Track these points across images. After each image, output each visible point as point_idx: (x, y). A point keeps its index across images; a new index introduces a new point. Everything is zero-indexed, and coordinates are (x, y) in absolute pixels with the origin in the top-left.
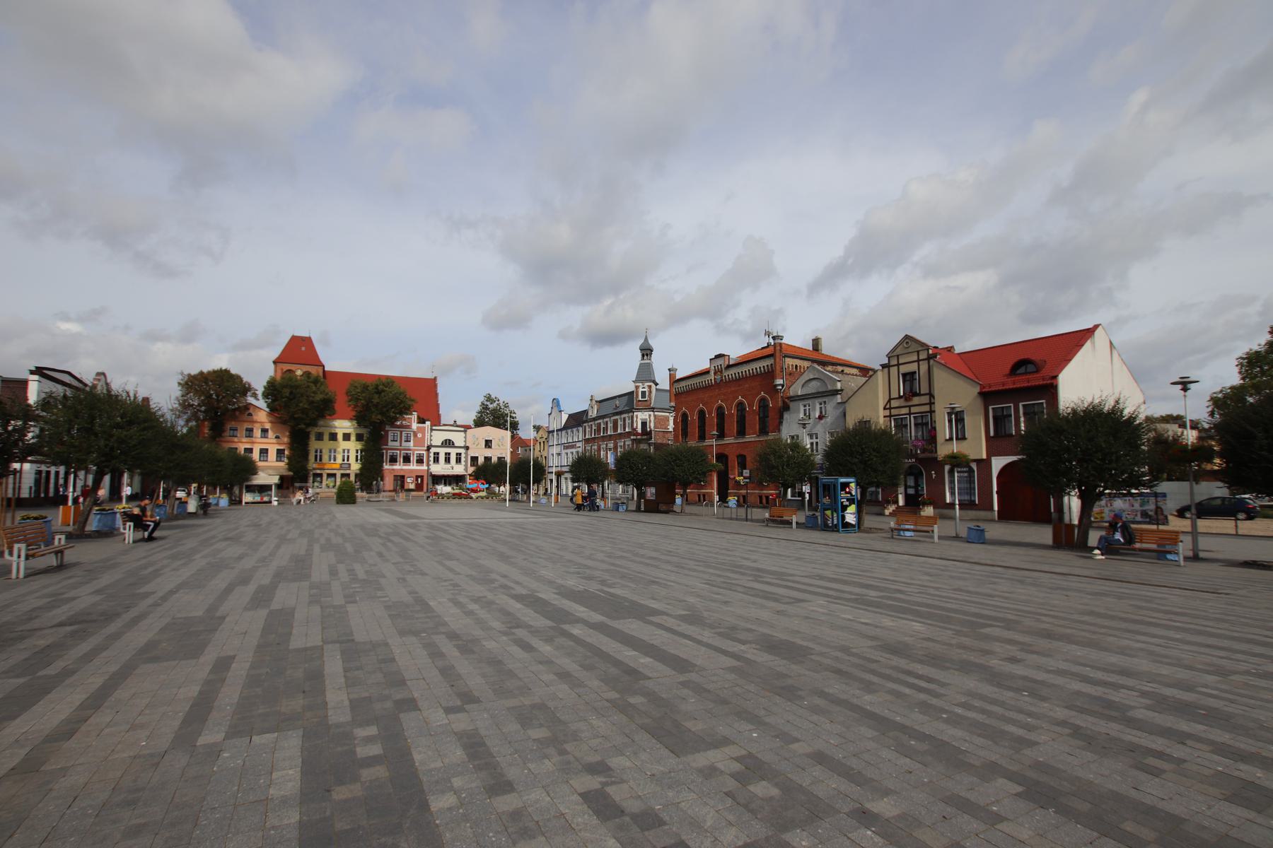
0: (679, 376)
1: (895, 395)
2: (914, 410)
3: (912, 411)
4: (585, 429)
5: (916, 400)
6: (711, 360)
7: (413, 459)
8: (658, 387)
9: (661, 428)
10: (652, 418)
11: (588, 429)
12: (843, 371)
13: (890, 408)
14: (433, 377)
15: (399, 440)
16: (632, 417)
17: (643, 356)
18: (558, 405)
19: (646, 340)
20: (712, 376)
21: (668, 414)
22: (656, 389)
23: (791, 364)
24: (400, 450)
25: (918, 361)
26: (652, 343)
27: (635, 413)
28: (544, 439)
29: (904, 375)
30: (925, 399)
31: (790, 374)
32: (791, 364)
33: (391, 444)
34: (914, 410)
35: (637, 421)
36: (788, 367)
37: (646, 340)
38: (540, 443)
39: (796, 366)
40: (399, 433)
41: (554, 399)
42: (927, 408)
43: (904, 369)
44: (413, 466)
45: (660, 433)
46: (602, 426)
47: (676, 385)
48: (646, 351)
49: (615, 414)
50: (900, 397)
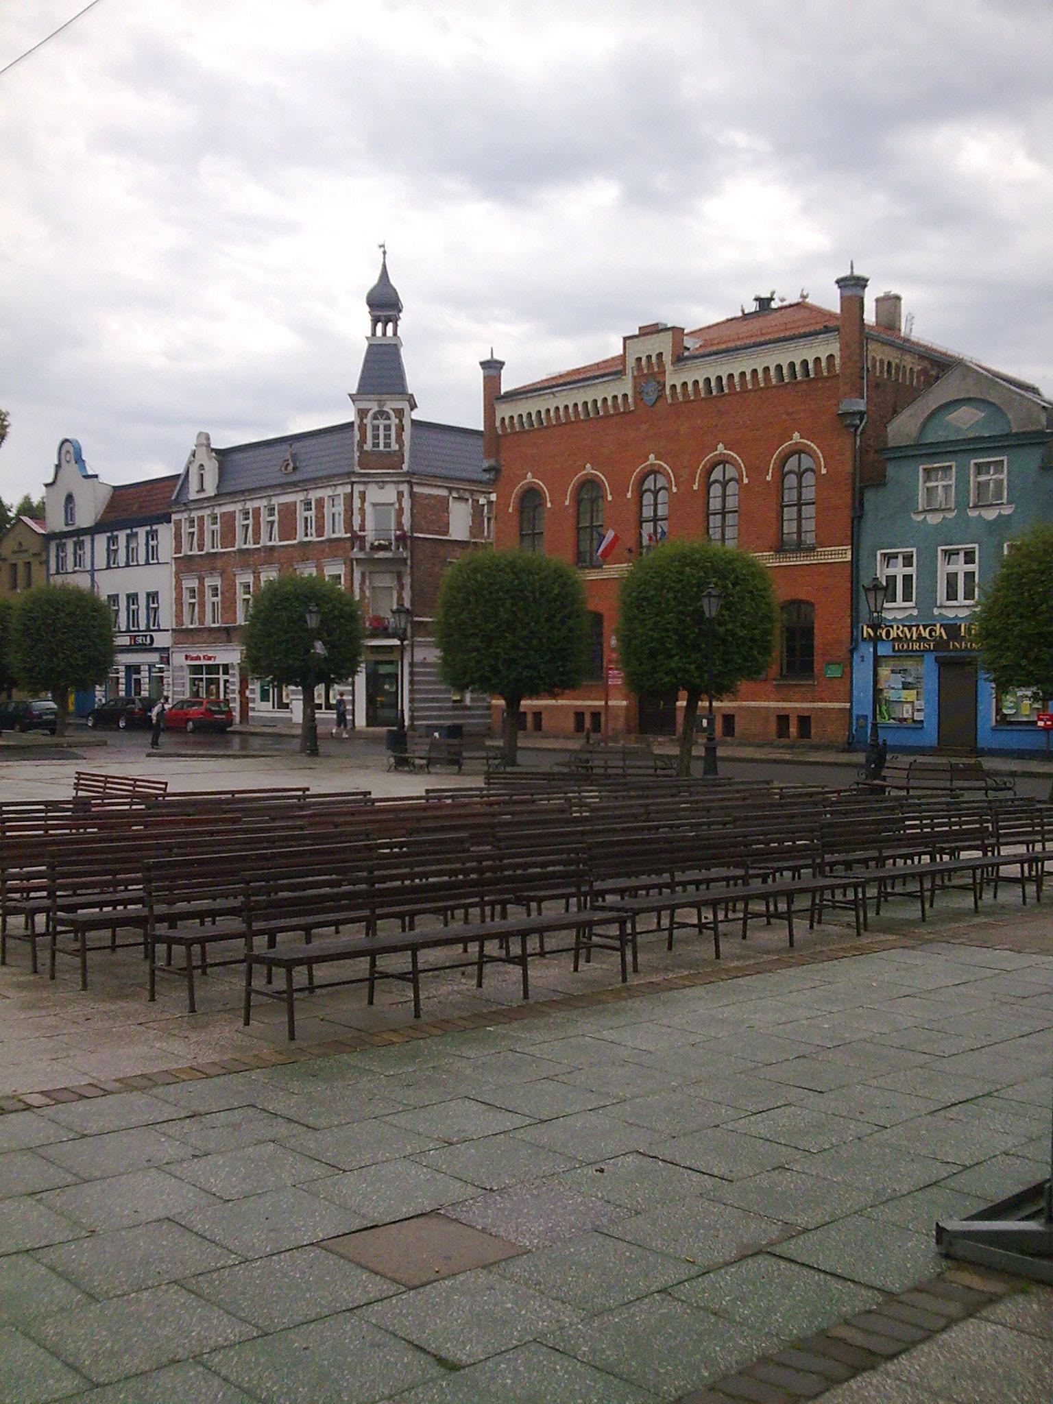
0: (508, 384)
6: (625, 339)
8: (416, 415)
10: (406, 503)
11: (185, 529)
16: (349, 498)
17: (375, 321)
18: (79, 460)
20: (625, 387)
21: (444, 493)
28: (26, 557)
31: (877, 386)
35: (362, 509)
36: (874, 366)
38: (14, 565)
46: (239, 521)
47: (504, 411)
49: (284, 487)
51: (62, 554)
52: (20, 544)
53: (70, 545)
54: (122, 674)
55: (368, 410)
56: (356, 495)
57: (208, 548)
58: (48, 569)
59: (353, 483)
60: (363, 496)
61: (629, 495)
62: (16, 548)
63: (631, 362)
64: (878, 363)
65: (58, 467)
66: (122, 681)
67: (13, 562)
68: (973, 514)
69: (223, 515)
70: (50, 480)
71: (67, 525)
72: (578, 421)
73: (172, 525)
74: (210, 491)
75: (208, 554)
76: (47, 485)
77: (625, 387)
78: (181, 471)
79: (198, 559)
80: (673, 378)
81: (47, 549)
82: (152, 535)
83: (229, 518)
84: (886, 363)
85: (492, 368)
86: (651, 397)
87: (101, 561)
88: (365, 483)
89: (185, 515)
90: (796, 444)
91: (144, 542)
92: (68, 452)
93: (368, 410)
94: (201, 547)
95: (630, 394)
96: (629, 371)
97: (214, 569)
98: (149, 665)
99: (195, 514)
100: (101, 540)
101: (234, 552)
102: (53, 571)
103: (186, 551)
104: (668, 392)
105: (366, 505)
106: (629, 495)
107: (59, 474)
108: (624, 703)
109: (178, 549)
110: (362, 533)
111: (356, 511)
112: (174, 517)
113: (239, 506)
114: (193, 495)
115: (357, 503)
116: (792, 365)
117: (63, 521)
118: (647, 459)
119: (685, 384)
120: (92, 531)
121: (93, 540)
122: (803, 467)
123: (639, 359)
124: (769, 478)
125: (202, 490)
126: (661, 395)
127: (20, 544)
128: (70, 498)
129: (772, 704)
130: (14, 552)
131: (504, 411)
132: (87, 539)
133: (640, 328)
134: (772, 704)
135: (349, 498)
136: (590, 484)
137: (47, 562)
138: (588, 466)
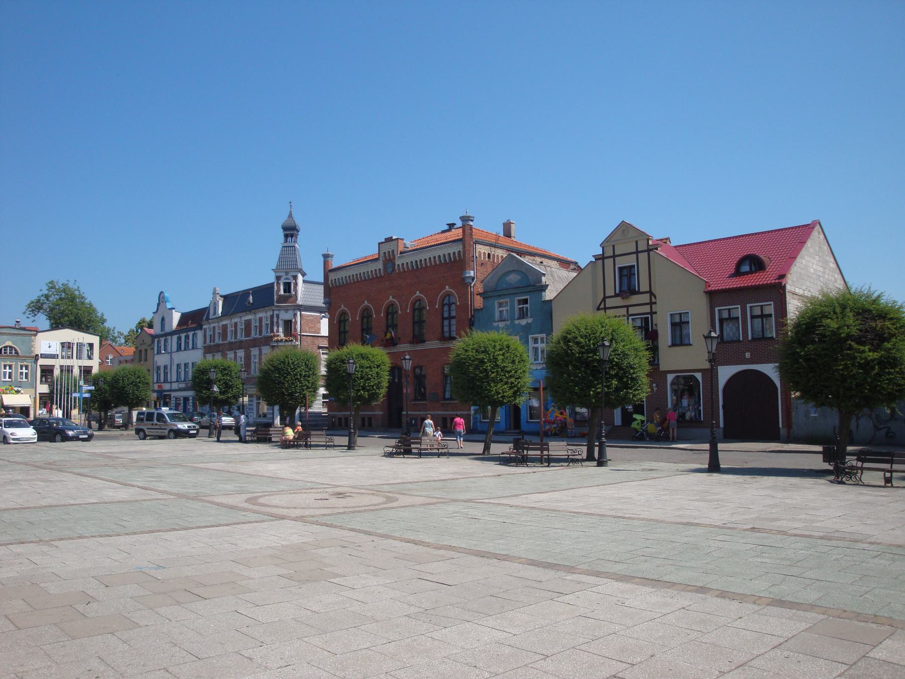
0: (335, 263)
1: (610, 292)
2: (632, 310)
3: (630, 312)
5: (635, 299)
6: (379, 244)
8: (306, 278)
9: (309, 332)
12: (541, 262)
13: (605, 309)
16: (272, 317)
17: (286, 236)
19: (290, 216)
20: (379, 265)
22: (304, 281)
23: (482, 251)
25: (637, 252)
26: (299, 221)
27: (276, 312)
29: (621, 269)
30: (645, 298)
31: (482, 264)
32: (482, 251)
34: (632, 310)
36: (480, 256)
37: (290, 216)
39: (489, 255)
42: (647, 309)
43: (622, 262)
45: (309, 338)
46: (229, 329)
47: (332, 276)
48: (290, 231)
50: (616, 295)
54: (182, 402)
55: (281, 277)
56: (275, 315)
58: (154, 353)
59: (273, 310)
60: (278, 316)
61: (382, 315)
63: (382, 254)
64: (482, 254)
66: (182, 405)
67: (140, 349)
68: (517, 322)
69: (223, 326)
70: (155, 310)
71: (162, 331)
72: (354, 282)
73: (203, 331)
76: (154, 313)
77: (379, 265)
78: (208, 306)
80: (398, 262)
81: (153, 342)
83: (225, 327)
84: (487, 254)
85: (326, 257)
86: (390, 270)
87: (175, 348)
88: (279, 310)
90: (447, 291)
93: (281, 277)
95: (381, 268)
96: (381, 258)
98: (176, 398)
100: (175, 338)
104: (396, 268)
105: (280, 320)
106: (382, 315)
107: (160, 308)
108: (381, 413)
109: (205, 342)
110: (278, 334)
111: (275, 323)
114: (211, 317)
115: (275, 319)
116: (449, 254)
117: (160, 330)
118: (389, 298)
119: (403, 264)
122: (451, 302)
123: (385, 253)
124: (437, 307)
126: (394, 269)
129: (440, 413)
130: (141, 344)
131: (332, 276)
132: (169, 337)
133: (385, 239)
134: (440, 413)
135: (272, 317)
136: (367, 309)
137: (153, 349)
138: (366, 302)
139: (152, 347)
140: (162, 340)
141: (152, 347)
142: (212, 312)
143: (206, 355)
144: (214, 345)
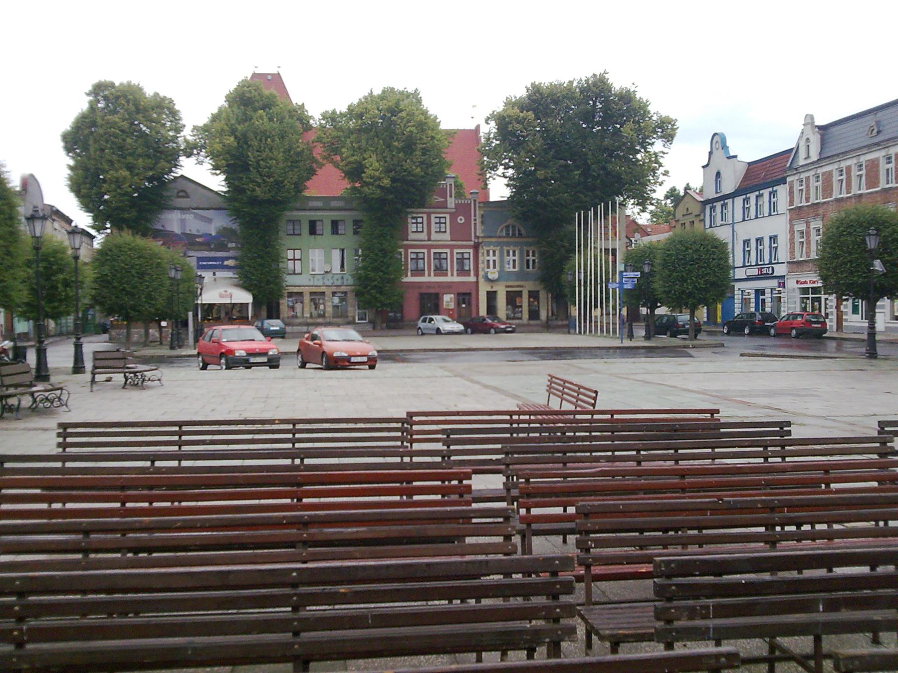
4: (791, 188)
7: (451, 265)
11: (797, 187)
14: (473, 128)
15: (425, 230)
18: (725, 147)
24: (429, 247)
33: (412, 236)
40: (425, 216)
41: (715, 134)
44: (452, 278)
46: (836, 177)
49: (870, 147)
51: (713, 214)
52: (687, 209)
53: (718, 205)
54: (753, 296)
57: (813, 200)
58: (705, 225)
62: (685, 213)
65: (710, 153)
66: (753, 300)
69: (824, 174)
70: (706, 163)
71: (717, 193)
74: (814, 157)
75: (813, 204)
76: (703, 167)
78: (792, 145)
79: (805, 209)
81: (703, 211)
82: (773, 194)
87: (739, 216)
89: (796, 177)
91: (768, 199)
92: (717, 142)
94: (807, 200)
97: (817, 215)
99: (803, 176)
100: (739, 201)
101: (832, 201)
102: (708, 226)
103: (797, 203)
109: (791, 202)
112: (788, 179)
113: (836, 166)
114: (801, 162)
120: (732, 196)
121: (733, 202)
125: (808, 157)
127: (687, 209)
128: (718, 174)
132: (729, 201)
137: (703, 220)
139: (702, 217)
140: (718, 205)
141: (702, 217)
142: (802, 154)
143: (794, 222)
144: (807, 206)
